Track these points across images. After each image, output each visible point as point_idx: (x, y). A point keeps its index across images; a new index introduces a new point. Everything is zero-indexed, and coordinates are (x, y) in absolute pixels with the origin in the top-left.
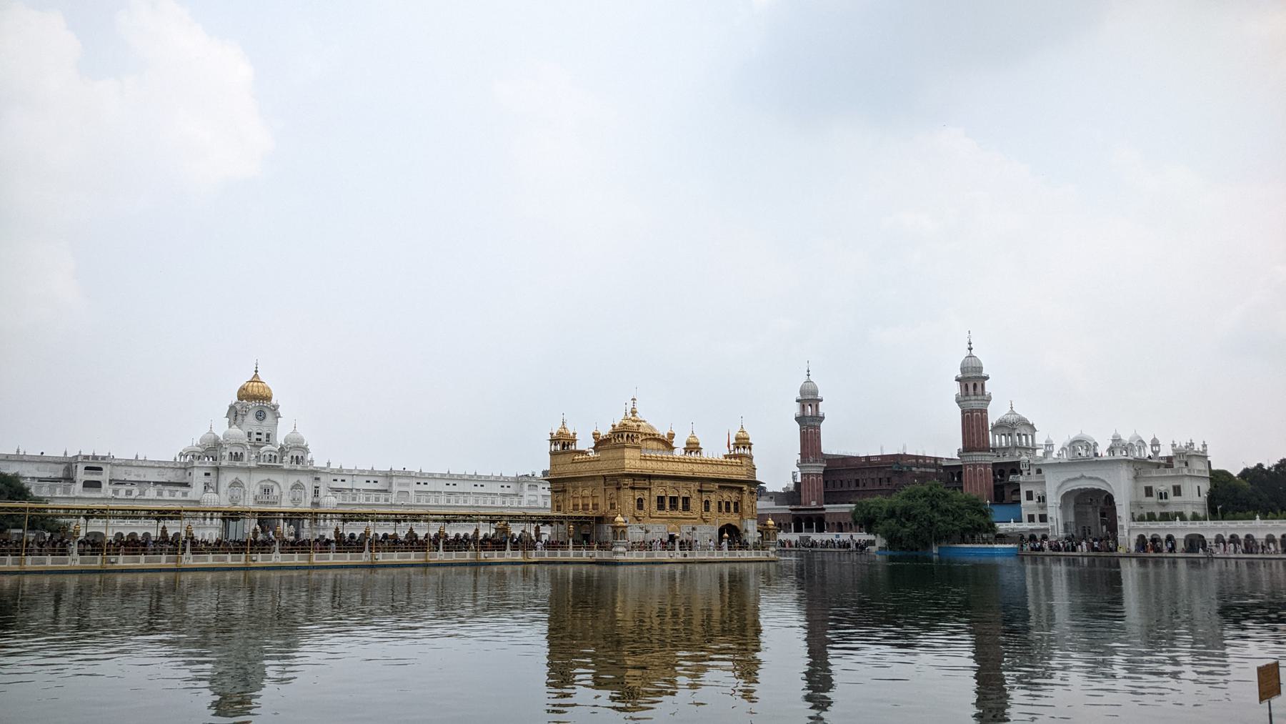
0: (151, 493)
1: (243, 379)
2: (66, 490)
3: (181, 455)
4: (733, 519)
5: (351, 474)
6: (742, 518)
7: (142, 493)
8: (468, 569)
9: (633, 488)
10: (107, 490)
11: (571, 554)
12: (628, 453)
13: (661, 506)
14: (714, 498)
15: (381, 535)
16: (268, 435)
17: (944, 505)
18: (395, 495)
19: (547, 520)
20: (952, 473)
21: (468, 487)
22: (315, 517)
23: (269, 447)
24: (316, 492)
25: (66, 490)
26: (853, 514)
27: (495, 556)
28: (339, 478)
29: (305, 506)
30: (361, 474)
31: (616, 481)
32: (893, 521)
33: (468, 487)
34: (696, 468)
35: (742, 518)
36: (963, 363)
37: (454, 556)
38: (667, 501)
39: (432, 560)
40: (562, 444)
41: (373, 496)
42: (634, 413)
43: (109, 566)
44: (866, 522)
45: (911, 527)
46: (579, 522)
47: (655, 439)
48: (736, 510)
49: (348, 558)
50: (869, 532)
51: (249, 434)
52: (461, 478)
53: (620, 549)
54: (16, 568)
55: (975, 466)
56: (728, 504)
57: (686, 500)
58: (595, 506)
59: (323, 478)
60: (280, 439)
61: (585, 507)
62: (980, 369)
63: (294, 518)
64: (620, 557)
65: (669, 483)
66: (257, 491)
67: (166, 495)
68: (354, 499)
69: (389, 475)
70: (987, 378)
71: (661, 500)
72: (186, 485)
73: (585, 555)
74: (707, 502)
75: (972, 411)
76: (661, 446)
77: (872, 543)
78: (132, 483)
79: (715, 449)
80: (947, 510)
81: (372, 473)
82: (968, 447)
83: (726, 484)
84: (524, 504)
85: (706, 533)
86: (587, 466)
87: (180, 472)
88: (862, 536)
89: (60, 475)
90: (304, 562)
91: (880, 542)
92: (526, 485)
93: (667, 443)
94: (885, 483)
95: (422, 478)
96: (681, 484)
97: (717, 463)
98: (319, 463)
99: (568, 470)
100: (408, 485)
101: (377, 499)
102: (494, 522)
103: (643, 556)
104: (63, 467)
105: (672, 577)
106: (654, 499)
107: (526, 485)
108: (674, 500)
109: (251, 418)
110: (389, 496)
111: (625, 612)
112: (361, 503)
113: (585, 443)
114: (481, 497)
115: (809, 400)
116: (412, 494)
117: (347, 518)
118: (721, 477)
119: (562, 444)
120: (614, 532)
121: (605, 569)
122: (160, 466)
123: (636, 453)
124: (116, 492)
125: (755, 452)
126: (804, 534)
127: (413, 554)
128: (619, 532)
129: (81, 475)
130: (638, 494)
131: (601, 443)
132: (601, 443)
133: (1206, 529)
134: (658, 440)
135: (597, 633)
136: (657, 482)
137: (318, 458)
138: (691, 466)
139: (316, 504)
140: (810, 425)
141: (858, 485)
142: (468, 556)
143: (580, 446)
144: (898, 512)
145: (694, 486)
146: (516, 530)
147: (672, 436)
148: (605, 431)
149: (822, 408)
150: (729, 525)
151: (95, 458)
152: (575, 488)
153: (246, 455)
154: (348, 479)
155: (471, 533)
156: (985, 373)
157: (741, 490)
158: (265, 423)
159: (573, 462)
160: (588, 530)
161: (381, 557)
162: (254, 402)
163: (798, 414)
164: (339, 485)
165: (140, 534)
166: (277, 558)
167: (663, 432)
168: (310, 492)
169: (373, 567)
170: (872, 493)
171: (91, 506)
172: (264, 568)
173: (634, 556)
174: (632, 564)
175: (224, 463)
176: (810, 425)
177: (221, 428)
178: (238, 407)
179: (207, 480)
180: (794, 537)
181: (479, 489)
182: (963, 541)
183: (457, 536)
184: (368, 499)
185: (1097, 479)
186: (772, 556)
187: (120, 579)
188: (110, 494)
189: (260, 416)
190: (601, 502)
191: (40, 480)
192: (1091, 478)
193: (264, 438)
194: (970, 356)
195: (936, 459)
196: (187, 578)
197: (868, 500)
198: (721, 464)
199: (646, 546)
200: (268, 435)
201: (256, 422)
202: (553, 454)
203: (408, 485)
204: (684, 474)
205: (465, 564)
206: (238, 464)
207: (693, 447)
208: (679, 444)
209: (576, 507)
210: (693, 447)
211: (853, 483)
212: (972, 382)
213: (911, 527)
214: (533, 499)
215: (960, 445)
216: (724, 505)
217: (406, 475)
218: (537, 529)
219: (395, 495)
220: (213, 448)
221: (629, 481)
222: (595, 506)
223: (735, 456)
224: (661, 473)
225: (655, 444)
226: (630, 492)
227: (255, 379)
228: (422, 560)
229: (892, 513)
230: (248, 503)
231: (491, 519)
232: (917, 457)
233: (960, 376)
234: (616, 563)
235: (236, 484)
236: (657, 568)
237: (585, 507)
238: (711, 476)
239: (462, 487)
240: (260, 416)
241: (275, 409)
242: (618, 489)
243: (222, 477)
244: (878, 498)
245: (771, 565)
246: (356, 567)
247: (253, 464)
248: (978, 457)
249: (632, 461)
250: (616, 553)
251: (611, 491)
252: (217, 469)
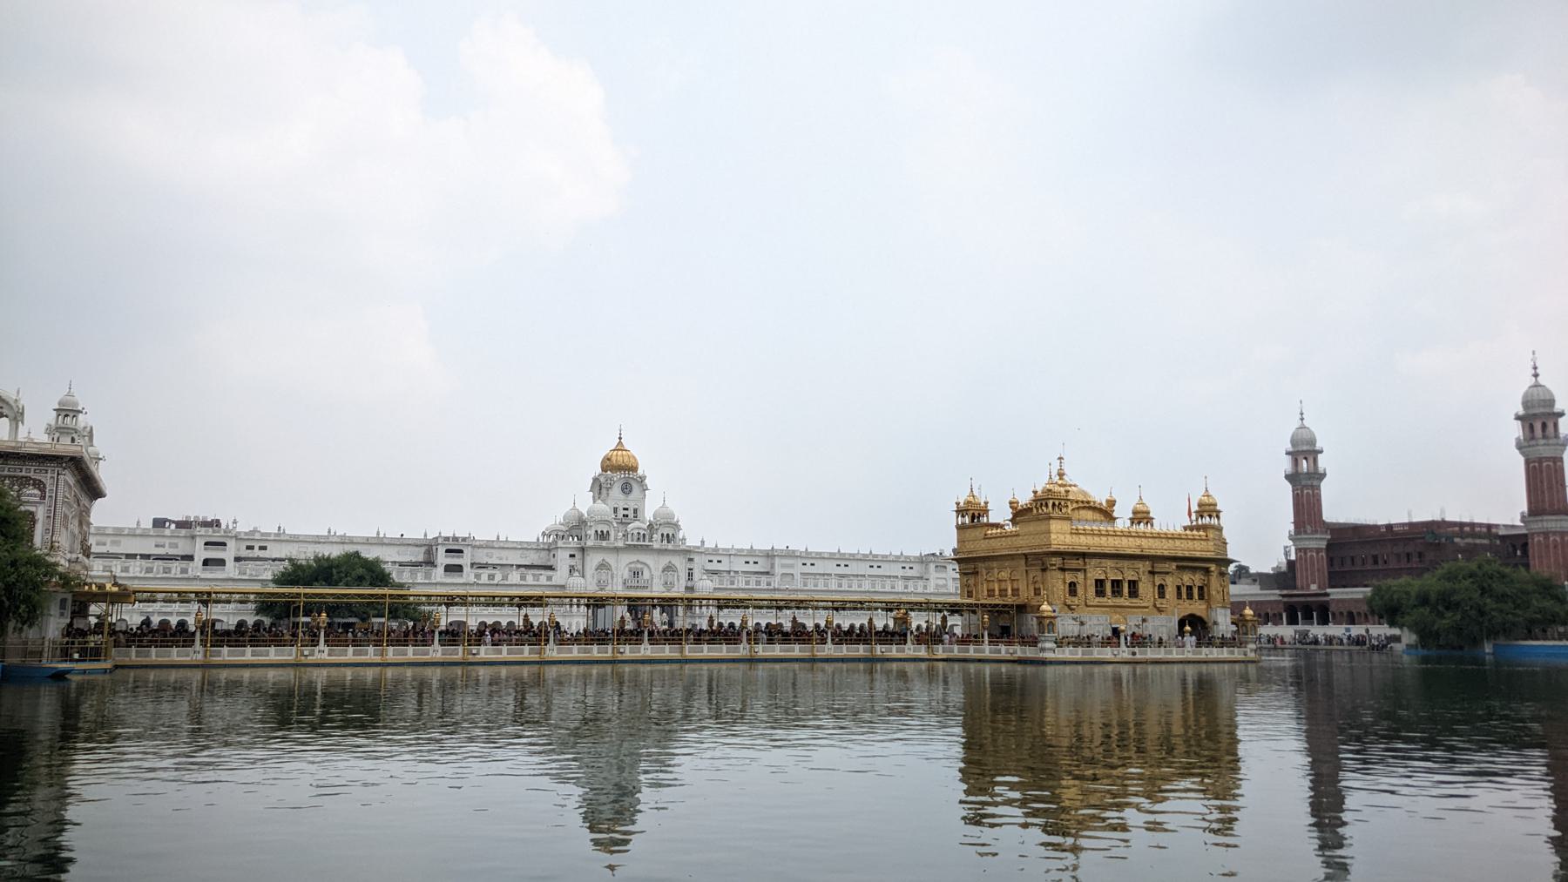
0: (514, 577)
1: (606, 447)
2: (428, 576)
3: (544, 534)
4: (1198, 608)
5: (729, 554)
6: (1209, 607)
7: (505, 578)
8: (862, 666)
9: (1063, 570)
10: (469, 575)
11: (987, 650)
12: (1055, 526)
13: (1100, 592)
14: (1170, 583)
15: (504, 624)
16: (635, 511)
17: (1498, 587)
18: (777, 579)
19: (955, 609)
20: (1513, 545)
21: (863, 569)
22: (689, 603)
23: (637, 524)
24: (690, 575)
25: (428, 576)
26: (1369, 601)
27: (893, 651)
28: (715, 559)
29: (678, 591)
30: (739, 553)
31: (1040, 560)
32: (1426, 611)
33: (863, 569)
34: (1144, 543)
35: (1209, 607)
36: (1526, 395)
37: (845, 651)
38: (1108, 586)
39: (820, 654)
40: (972, 515)
41: (753, 579)
42: (1061, 475)
43: (471, 658)
44: (1390, 612)
45: (1450, 619)
46: (996, 611)
47: (1090, 508)
48: (1201, 597)
49: (723, 651)
50: (1392, 624)
51: (615, 510)
52: (853, 558)
53: (1048, 645)
54: (378, 659)
55: (1546, 534)
56: (1189, 588)
57: (1133, 584)
58: (1015, 592)
59: (697, 558)
60: (649, 515)
61: (1003, 593)
62: (1552, 402)
63: (667, 604)
64: (1049, 655)
65: (1109, 563)
66: (626, 575)
67: (530, 580)
68: (732, 583)
69: (770, 555)
70: (1561, 414)
71: (1100, 584)
72: (550, 568)
73: (1004, 651)
74: (1161, 587)
75: (1540, 461)
76: (1098, 516)
77: (1397, 639)
78: (494, 566)
79: (1171, 518)
80: (1504, 595)
81: (752, 552)
82: (1537, 508)
83: (1186, 563)
84: (931, 589)
85: (1163, 625)
86: (1005, 542)
87: (543, 554)
88: (1380, 631)
89: (421, 558)
90: (676, 655)
91: (1408, 637)
92: (932, 566)
93: (1106, 513)
94: (1415, 559)
95: (807, 557)
96: (1126, 563)
97: (1173, 537)
98: (692, 542)
99: (981, 548)
100: (792, 566)
101: (758, 583)
102: (891, 610)
103: (1079, 654)
104: (423, 549)
105: (1117, 680)
106: (1091, 582)
107: (932, 566)
108: (1117, 584)
109: (616, 491)
110: (771, 579)
111: (1057, 720)
112: (740, 587)
113: (1000, 514)
114: (878, 581)
116: (798, 577)
117: (722, 604)
118: (1180, 554)
119: (972, 515)
120: (1040, 623)
121: (1030, 669)
122: (523, 547)
123: (1066, 526)
124: (478, 576)
125: (1225, 521)
126: (1300, 627)
127: (797, 647)
128: (1046, 624)
129: (442, 559)
130: (1069, 577)
131: (1020, 514)
132: (1020, 514)
134: (1094, 509)
135: (1022, 748)
136: (1094, 562)
137: (691, 536)
138: (1138, 541)
139: (690, 589)
140: (1305, 485)
141: (1376, 562)
142: (861, 650)
143: (993, 518)
144: (1433, 597)
145: (1144, 567)
146: (918, 620)
147: (1112, 503)
148: (1025, 499)
149: (1323, 462)
150: (1192, 616)
151: (455, 539)
152: (989, 570)
153: (612, 534)
154: (725, 560)
155: (738, 623)
156: (1558, 407)
157: (1207, 571)
158: (631, 497)
159: (986, 537)
160: (1006, 622)
161: (762, 650)
162: (619, 473)
164: (714, 566)
165: (174, 621)
166: (646, 650)
167: (1100, 498)
168: (683, 575)
169: (752, 661)
170: (1397, 573)
171: (184, 588)
172: (633, 662)
173: (1067, 653)
174: (1065, 663)
175: (590, 543)
176: (1305, 485)
177: (585, 503)
178: (602, 479)
179: (572, 562)
180: (1286, 631)
181: (875, 571)
182: (1530, 635)
183: (852, 626)
184: (747, 583)
186: (1252, 655)
187: (224, 675)
188: (472, 579)
189: (626, 489)
190: (1022, 586)
191: (401, 564)
193: (631, 513)
194: (1537, 385)
195: (1489, 526)
196: (551, 672)
197: (1390, 582)
198: (1179, 537)
199: (1078, 642)
200: (635, 511)
201: (622, 496)
202: (960, 528)
203: (792, 566)
204: (1129, 551)
205: (859, 660)
206: (604, 543)
207: (1141, 517)
208: (1123, 515)
209: (991, 593)
210: (1141, 517)
211: (1370, 561)
212: (1538, 418)
213: (1450, 619)
214: (941, 582)
215: (1525, 508)
216: (1184, 590)
217: (790, 554)
218: (944, 619)
219: (777, 579)
220: (577, 526)
221: (1057, 561)
222: (1015, 592)
223: (1198, 528)
224: (1099, 550)
225: (1089, 514)
226: (1059, 575)
227: (620, 447)
228: (807, 654)
229: (1424, 600)
230: (617, 588)
231: (889, 607)
232: (1462, 525)
233: (1521, 411)
234: (1044, 662)
235: (603, 566)
236: (1096, 669)
237: (1003, 593)
238: (1166, 553)
239: (854, 568)
240: (626, 489)
241: (643, 479)
242: (1044, 570)
243: (588, 559)
244: (1403, 580)
245: (1252, 668)
246: (733, 661)
247: (620, 544)
248: (1552, 523)
249: (1060, 535)
250: (1043, 650)
251: (1035, 573)
252: (583, 550)
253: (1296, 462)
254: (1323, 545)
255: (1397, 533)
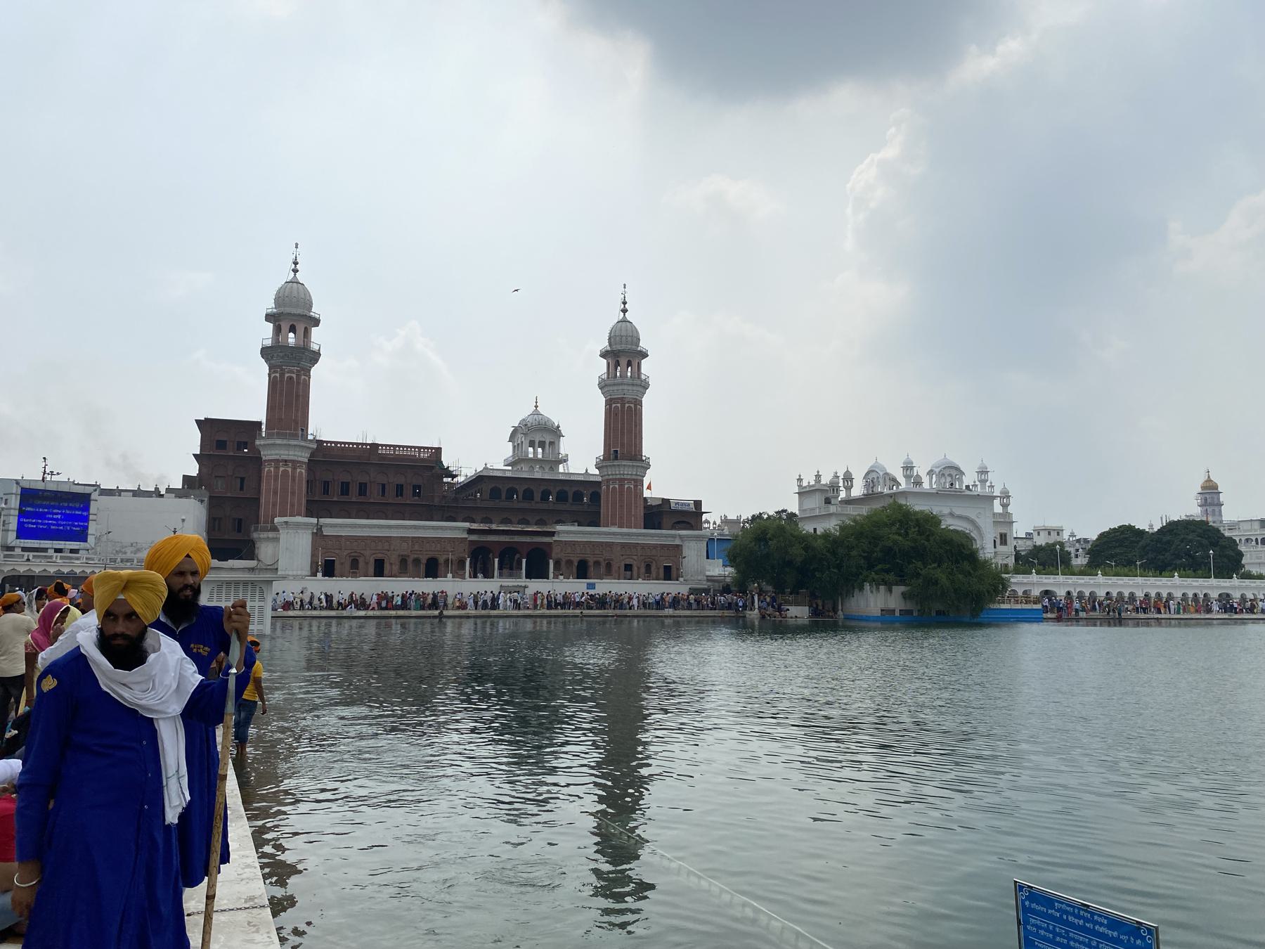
55: (622, 480)
115: (292, 317)
133: (1059, 585)
140: (290, 365)
163: (269, 343)
185: (967, 519)
192: (960, 517)
194: (624, 321)
253: (278, 330)
254: (304, 457)
255: (383, 457)
